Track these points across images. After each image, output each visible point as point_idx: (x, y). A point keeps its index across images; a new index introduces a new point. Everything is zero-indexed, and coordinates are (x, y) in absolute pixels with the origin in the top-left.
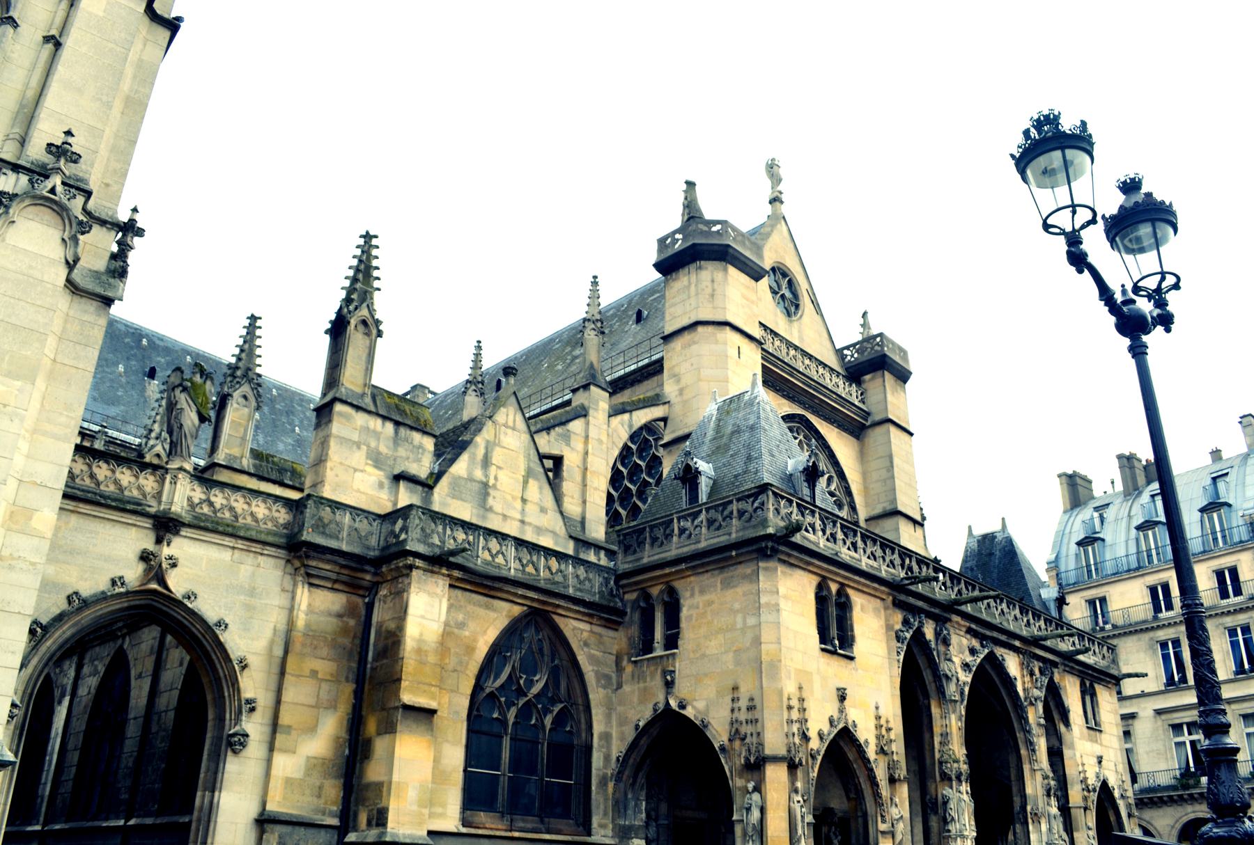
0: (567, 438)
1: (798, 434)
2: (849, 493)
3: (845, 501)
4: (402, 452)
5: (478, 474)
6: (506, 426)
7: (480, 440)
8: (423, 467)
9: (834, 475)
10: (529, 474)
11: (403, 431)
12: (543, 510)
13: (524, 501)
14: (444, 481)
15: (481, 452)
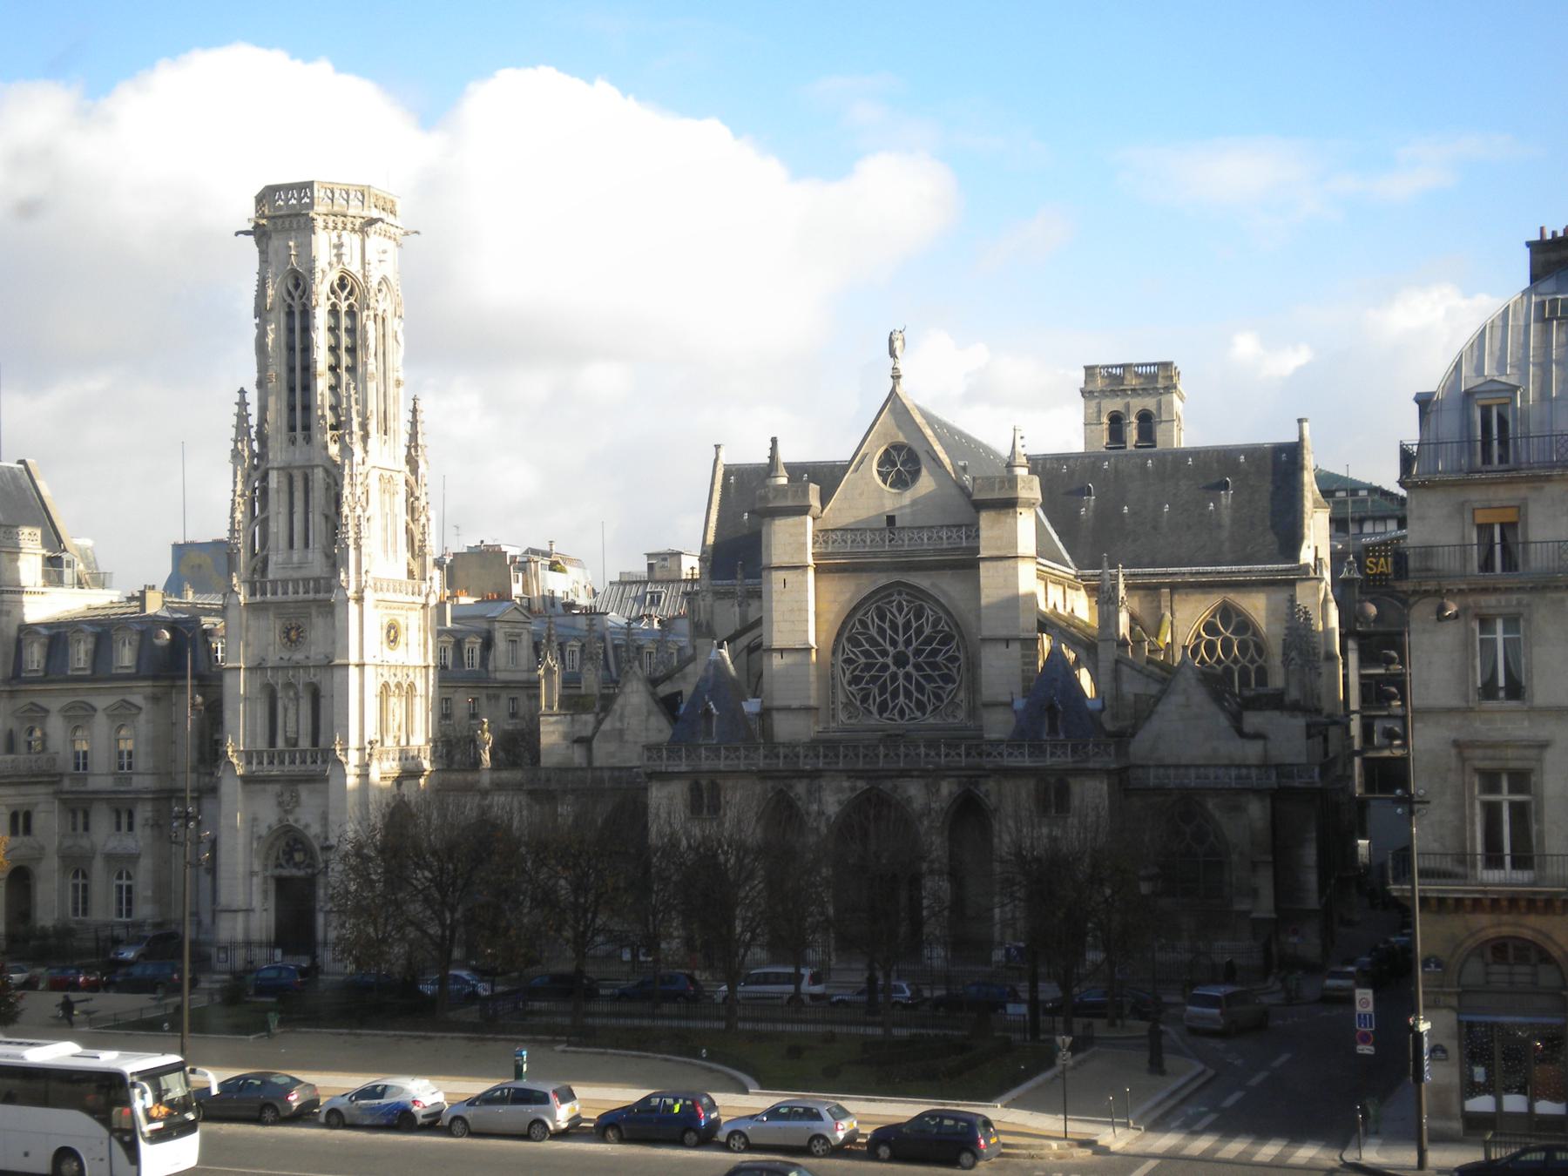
0: (684, 678)
1: (900, 593)
2: (957, 625)
3: (955, 633)
4: (577, 727)
5: (618, 725)
6: (632, 692)
7: (616, 707)
8: (588, 732)
9: (941, 614)
10: (649, 713)
11: (576, 717)
12: (661, 731)
13: (647, 729)
14: (598, 735)
15: (618, 713)
